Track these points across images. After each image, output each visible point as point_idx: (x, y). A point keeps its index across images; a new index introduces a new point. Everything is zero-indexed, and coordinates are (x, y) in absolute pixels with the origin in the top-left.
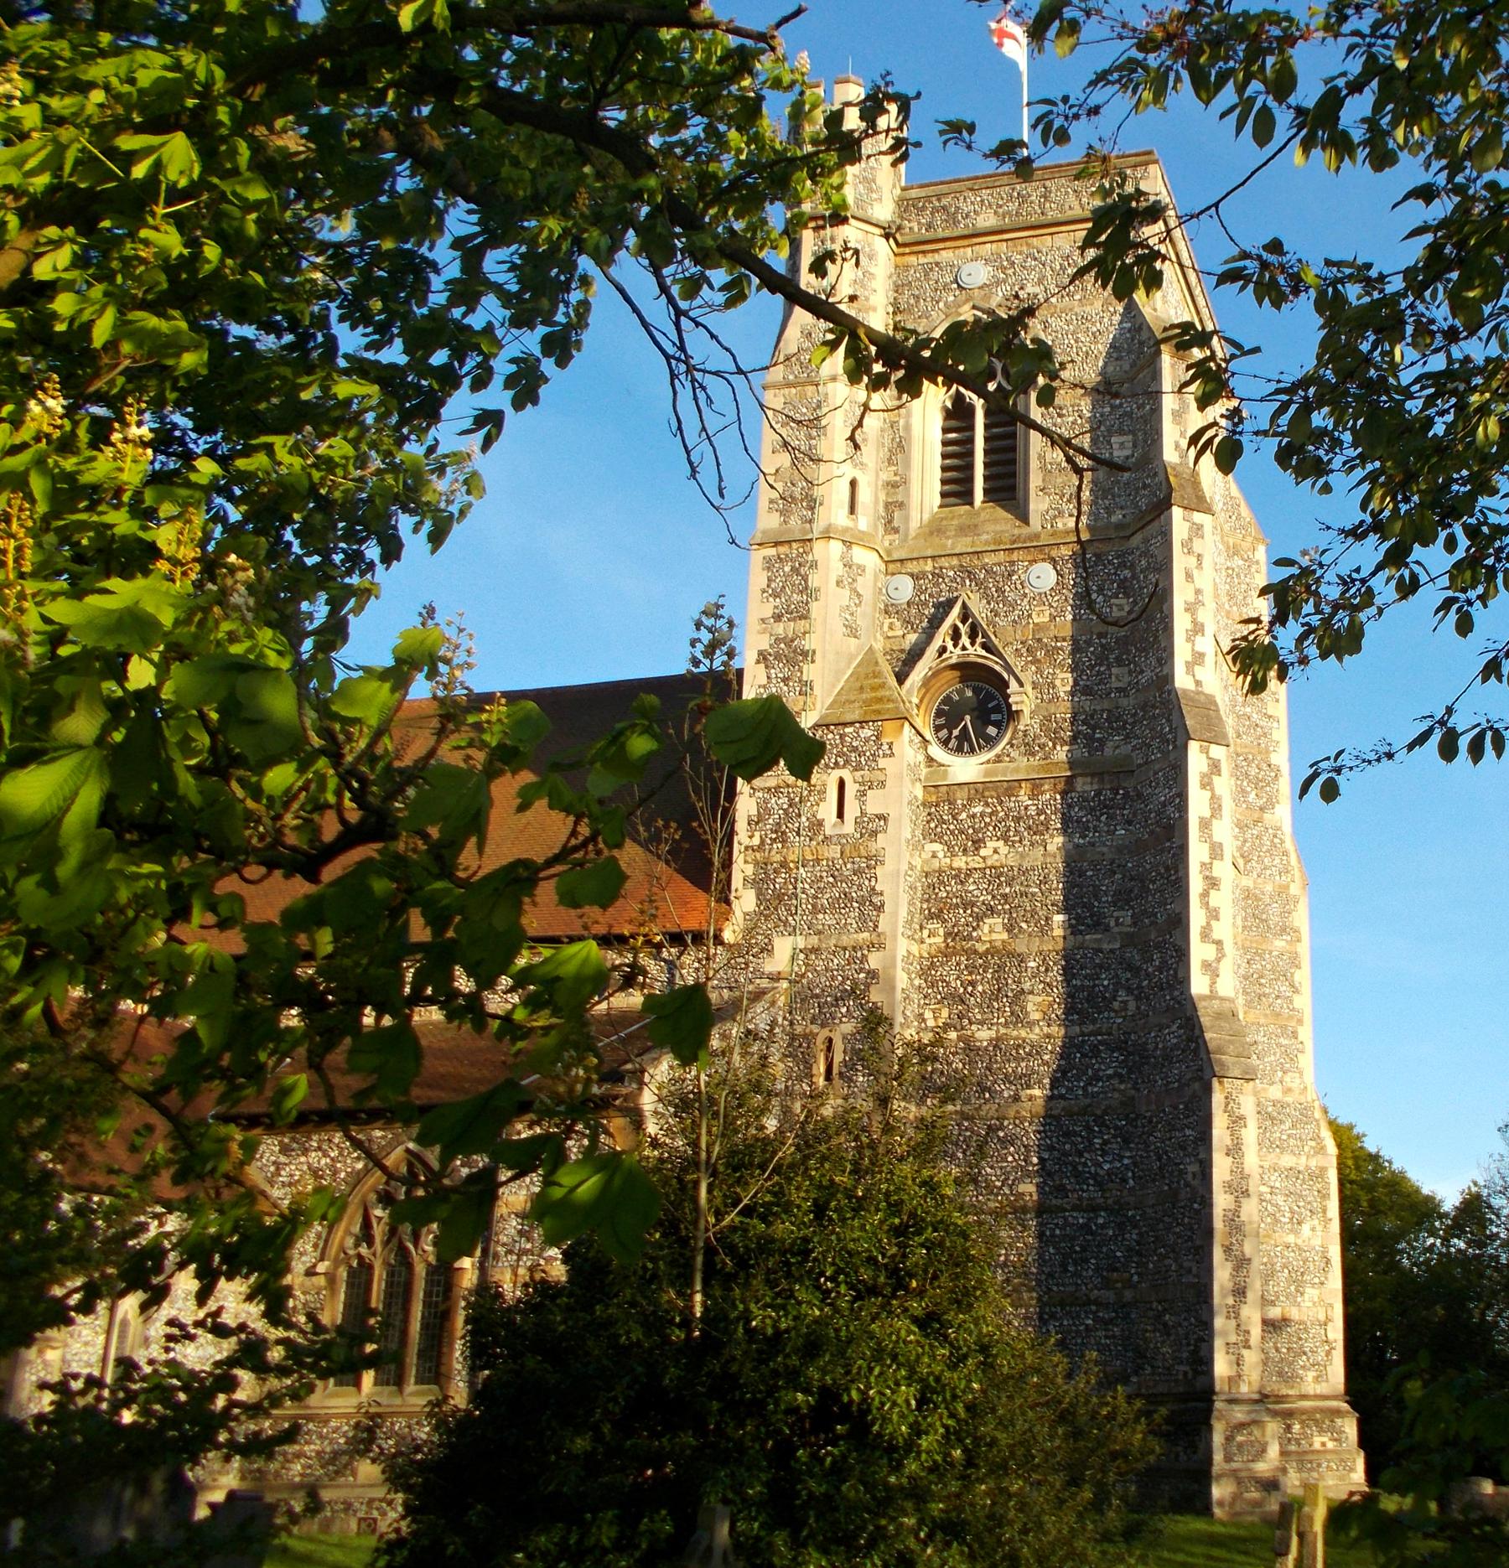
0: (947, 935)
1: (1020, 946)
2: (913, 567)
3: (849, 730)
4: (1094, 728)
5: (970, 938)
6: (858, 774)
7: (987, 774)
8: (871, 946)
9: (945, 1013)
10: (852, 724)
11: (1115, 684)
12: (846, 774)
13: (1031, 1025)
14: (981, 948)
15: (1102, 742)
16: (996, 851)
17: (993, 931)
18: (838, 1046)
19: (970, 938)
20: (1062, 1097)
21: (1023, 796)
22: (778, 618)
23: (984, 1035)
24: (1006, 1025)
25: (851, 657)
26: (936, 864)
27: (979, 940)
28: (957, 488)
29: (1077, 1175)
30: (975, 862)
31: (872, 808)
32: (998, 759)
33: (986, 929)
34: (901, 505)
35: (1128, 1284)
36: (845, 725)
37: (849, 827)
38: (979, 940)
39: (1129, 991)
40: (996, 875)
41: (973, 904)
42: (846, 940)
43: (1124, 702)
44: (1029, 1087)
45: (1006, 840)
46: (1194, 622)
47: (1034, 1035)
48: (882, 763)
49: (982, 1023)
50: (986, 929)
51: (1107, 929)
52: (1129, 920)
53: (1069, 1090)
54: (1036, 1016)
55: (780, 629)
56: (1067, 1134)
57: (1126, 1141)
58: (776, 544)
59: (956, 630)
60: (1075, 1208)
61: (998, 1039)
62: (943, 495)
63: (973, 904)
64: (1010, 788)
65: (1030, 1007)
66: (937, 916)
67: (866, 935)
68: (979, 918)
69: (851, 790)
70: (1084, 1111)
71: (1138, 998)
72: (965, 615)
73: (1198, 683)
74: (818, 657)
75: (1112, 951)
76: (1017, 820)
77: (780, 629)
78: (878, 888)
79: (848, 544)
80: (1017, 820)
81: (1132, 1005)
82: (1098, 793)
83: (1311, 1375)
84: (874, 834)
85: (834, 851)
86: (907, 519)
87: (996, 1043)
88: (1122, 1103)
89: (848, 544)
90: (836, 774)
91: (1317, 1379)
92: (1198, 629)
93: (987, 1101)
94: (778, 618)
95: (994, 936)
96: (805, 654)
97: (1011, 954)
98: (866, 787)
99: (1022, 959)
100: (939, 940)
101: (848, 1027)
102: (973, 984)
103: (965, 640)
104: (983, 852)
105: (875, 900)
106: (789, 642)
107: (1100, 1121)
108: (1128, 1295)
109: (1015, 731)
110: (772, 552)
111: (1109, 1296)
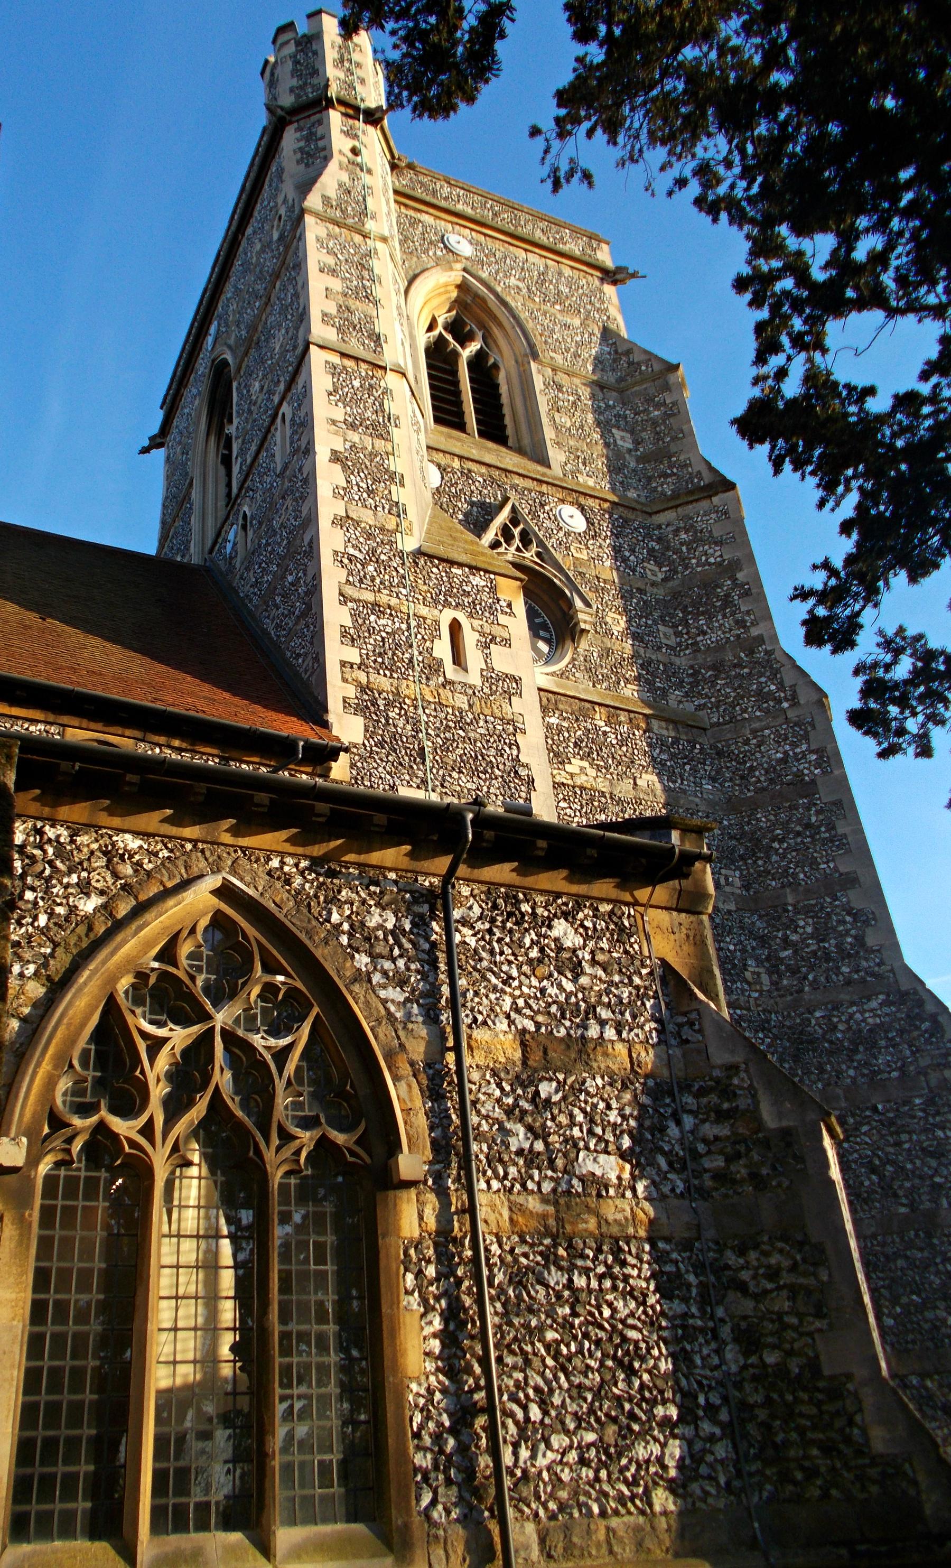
3: (456, 571)
6: (476, 623)
10: (461, 565)
12: (461, 617)
15: (664, 693)
32: (562, 675)
36: (452, 563)
37: (474, 678)
52: (738, 883)
58: (344, 355)
64: (585, 708)
69: (470, 638)
77: (354, 437)
82: (676, 741)
94: (353, 427)
96: (392, 476)
98: (487, 642)
104: (568, 767)
105: (523, 772)
110: (335, 359)
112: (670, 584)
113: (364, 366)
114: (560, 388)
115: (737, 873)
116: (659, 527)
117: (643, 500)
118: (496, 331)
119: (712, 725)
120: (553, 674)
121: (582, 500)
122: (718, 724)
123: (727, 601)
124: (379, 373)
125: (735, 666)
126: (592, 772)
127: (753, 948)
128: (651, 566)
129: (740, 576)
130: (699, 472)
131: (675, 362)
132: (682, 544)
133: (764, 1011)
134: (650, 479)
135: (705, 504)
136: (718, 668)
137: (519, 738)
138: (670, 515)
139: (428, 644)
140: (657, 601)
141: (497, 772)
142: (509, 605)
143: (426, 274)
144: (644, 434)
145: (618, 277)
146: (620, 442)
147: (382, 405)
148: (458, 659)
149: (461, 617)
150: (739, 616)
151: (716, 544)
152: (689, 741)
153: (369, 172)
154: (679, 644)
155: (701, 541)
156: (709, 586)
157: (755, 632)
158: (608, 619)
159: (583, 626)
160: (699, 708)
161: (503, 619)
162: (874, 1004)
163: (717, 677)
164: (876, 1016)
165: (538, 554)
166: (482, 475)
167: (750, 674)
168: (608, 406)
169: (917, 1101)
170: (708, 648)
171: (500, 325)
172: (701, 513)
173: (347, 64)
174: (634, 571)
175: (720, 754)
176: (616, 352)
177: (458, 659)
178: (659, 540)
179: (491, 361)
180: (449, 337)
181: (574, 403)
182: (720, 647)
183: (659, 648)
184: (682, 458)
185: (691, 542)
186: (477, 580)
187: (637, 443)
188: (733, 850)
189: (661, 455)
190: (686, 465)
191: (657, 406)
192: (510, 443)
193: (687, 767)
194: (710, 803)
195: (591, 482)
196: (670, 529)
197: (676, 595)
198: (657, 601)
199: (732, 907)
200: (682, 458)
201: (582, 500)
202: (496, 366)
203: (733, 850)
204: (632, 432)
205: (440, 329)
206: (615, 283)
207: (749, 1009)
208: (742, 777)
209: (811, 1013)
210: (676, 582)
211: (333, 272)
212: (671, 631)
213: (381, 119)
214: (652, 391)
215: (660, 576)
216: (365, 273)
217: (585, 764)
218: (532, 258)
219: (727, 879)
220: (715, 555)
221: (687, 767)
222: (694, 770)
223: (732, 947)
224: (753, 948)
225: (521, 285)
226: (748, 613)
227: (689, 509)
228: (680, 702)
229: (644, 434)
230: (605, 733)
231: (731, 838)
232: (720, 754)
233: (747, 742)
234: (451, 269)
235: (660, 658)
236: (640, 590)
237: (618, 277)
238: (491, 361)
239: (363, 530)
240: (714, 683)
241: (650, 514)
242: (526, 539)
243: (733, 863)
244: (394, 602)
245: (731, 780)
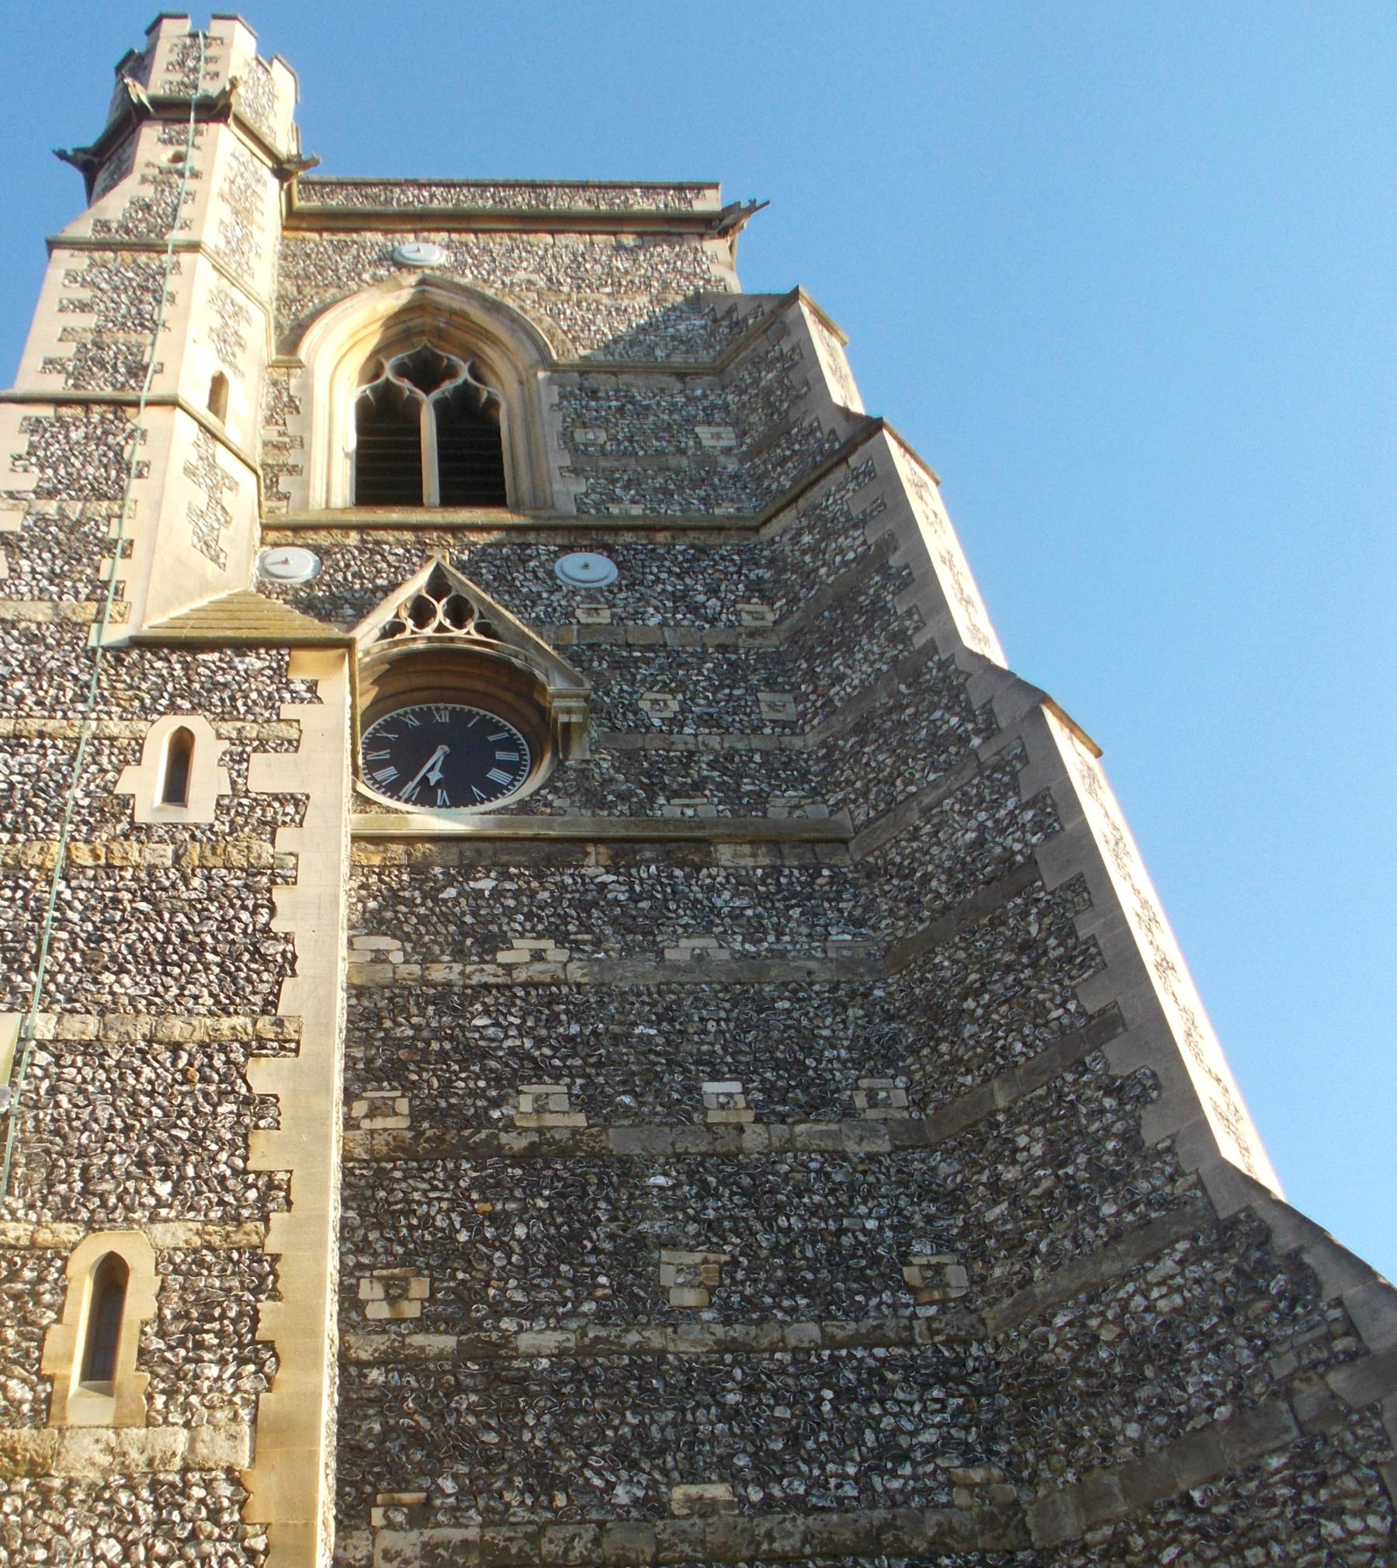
0: (415, 1116)
1: (619, 1140)
2: (323, 539)
4: (738, 776)
5: (481, 1119)
6: (228, 728)
7: (500, 825)
8: (255, 1047)
9: (420, 1288)
12: (199, 725)
13: (676, 1319)
14: (515, 1142)
15: (761, 799)
16: (538, 956)
17: (544, 1109)
19: (481, 1119)
20: (797, 1504)
21: (595, 867)
24: (602, 1317)
25: (205, 587)
26: (385, 974)
27: (510, 1125)
30: (490, 974)
32: (524, 808)
33: (526, 1104)
34: (293, 470)
38: (510, 1125)
39: (942, 1242)
40: (544, 999)
41: (484, 1055)
42: (176, 1028)
44: (692, 1476)
45: (562, 939)
47: (688, 1344)
48: (288, 711)
49: (530, 1312)
50: (526, 1104)
51: (849, 1112)
52: (901, 1097)
53: (813, 1484)
54: (690, 1298)
61: (582, 1351)
63: (484, 1055)
65: (668, 1276)
66: (394, 1073)
67: (238, 1021)
68: (507, 1083)
71: (966, 1260)
74: (137, 551)
75: (872, 1157)
76: (585, 907)
77: (51, 508)
78: (277, 926)
80: (585, 907)
81: (957, 1277)
82: (774, 871)
86: (306, 486)
87: (576, 1365)
88: (988, 1521)
90: (169, 725)
93: (561, 1518)
95: (549, 1120)
100: (398, 1123)
101: (176, 1233)
102: (501, 1221)
104: (503, 957)
105: (270, 948)
109: (559, 767)
110: (47, 412)
112: (787, 623)
113: (96, 408)
114: (593, 394)
115: (901, 1081)
116: (772, 542)
117: (747, 513)
118: (491, 353)
119: (857, 830)
120: (504, 810)
121: (608, 539)
122: (869, 822)
123: (877, 608)
124: (130, 411)
125: (890, 712)
126: (556, 954)
127: (929, 1219)
128: (756, 604)
129: (895, 560)
130: (833, 432)
131: (787, 290)
132: (804, 553)
133: (949, 1343)
134: (758, 480)
135: (839, 474)
136: (861, 729)
137: (280, 895)
138: (788, 517)
139: (110, 776)
140: (760, 658)
141: (210, 957)
142: (312, 687)
143: (348, 303)
144: (754, 418)
145: (727, 221)
146: (707, 442)
147: (119, 454)
148: (176, 790)
149: (199, 725)
150: (895, 626)
151: (855, 527)
152: (802, 868)
153: (195, 175)
154: (803, 715)
155: (827, 536)
156: (844, 599)
157: (919, 641)
158: (644, 705)
159: (563, 718)
160: (836, 808)
161: (288, 711)
162: (1168, 1265)
163: (863, 743)
164: (1173, 1290)
165: (479, 628)
166: (402, 544)
167: (916, 715)
168: (690, 400)
169: (1275, 1462)
170: (849, 700)
171: (494, 341)
172: (837, 494)
173: (190, 63)
174: (713, 621)
175: (871, 873)
176: (715, 321)
177: (176, 790)
178: (771, 562)
179: (484, 396)
180: (405, 384)
181: (621, 410)
182: (866, 690)
183: (757, 729)
184: (805, 424)
185: (818, 542)
186: (252, 662)
187: (741, 435)
188: (895, 1038)
189: (780, 431)
190: (812, 431)
191: (770, 365)
192: (509, 500)
193: (795, 913)
194: (848, 966)
195: (636, 510)
196: (786, 538)
197: (795, 637)
198: (760, 658)
199: (884, 1146)
200: (805, 424)
201: (608, 539)
202: (493, 403)
203: (895, 1038)
204: (735, 424)
205: (388, 374)
206: (723, 233)
207: (908, 1344)
208: (909, 901)
209: (1047, 1322)
210: (797, 615)
211: (84, 307)
212: (788, 697)
213: (228, 107)
214: (761, 351)
215: (771, 617)
216: (148, 297)
217: (548, 944)
218: (563, 239)
219: (871, 1094)
220: (852, 545)
221: (795, 913)
222: (811, 915)
223: (871, 1224)
224: (929, 1219)
225: (534, 277)
226: (909, 613)
227: (815, 495)
228: (798, 807)
229: (754, 418)
230: (604, 886)
231: (889, 1017)
232: (871, 873)
233: (915, 835)
234: (401, 287)
235: (756, 743)
236: (722, 648)
237: (727, 221)
238: (484, 396)
239: (25, 633)
240: (857, 755)
241: (756, 529)
242: (459, 613)
243: (890, 1063)
244: (51, 726)
245: (891, 912)
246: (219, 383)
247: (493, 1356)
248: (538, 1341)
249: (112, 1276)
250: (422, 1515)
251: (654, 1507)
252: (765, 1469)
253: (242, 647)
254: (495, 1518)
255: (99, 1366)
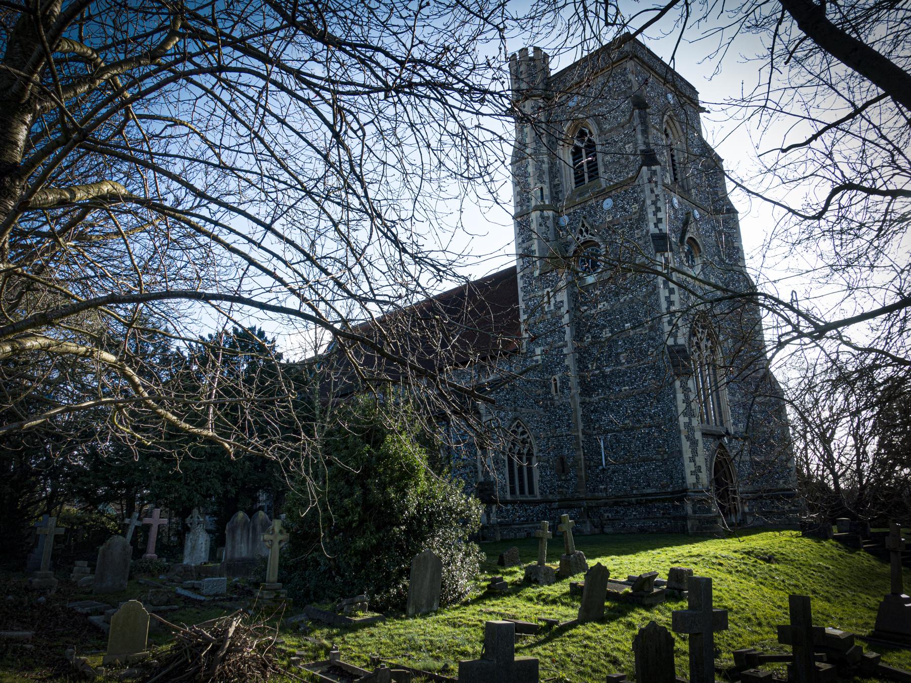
0: (592, 337)
11: (637, 236)
17: (606, 334)
18: (558, 382)
22: (523, 242)
23: (608, 370)
28: (579, 180)
29: (643, 415)
31: (558, 299)
35: (665, 452)
37: (552, 308)
40: (605, 313)
42: (557, 345)
43: (641, 242)
45: (606, 300)
46: (656, 207)
47: (623, 368)
55: (524, 245)
56: (639, 401)
57: (658, 401)
59: (581, 230)
60: (644, 427)
62: (576, 183)
68: (601, 330)
70: (643, 392)
72: (583, 226)
73: (660, 230)
77: (524, 245)
79: (542, 211)
83: (781, 482)
84: (560, 308)
85: (549, 316)
89: (542, 211)
91: (785, 483)
92: (658, 210)
97: (613, 341)
99: (617, 342)
101: (560, 375)
103: (585, 234)
106: (527, 249)
107: (648, 395)
108: (666, 456)
111: (659, 457)
246: (542, 189)
247: (603, 373)
248: (608, 370)
249: (555, 380)
250: (598, 395)
251: (620, 391)
252: (632, 384)
253: (552, 271)
254: (605, 394)
255: (556, 392)
